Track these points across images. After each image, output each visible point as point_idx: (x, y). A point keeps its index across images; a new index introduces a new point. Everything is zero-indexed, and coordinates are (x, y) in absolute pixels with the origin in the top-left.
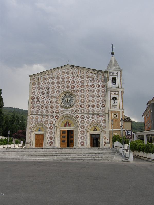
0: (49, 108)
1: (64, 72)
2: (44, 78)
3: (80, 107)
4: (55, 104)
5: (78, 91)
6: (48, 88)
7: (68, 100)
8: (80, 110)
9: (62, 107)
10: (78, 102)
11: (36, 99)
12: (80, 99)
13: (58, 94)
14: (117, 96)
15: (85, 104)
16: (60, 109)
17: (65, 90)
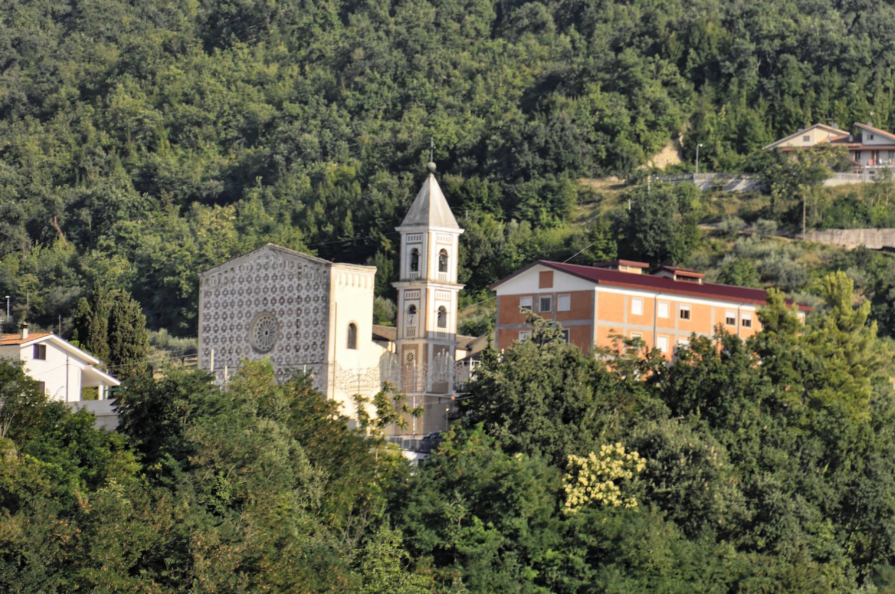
0: (234, 354)
1: (259, 264)
2: (226, 278)
3: (284, 351)
4: (243, 345)
5: (282, 313)
6: (232, 304)
7: (267, 333)
8: (284, 357)
9: (256, 350)
10: (281, 339)
11: (212, 332)
12: (285, 331)
13: (248, 318)
14: (416, 303)
15: (293, 342)
16: (253, 356)
17: (261, 308)
